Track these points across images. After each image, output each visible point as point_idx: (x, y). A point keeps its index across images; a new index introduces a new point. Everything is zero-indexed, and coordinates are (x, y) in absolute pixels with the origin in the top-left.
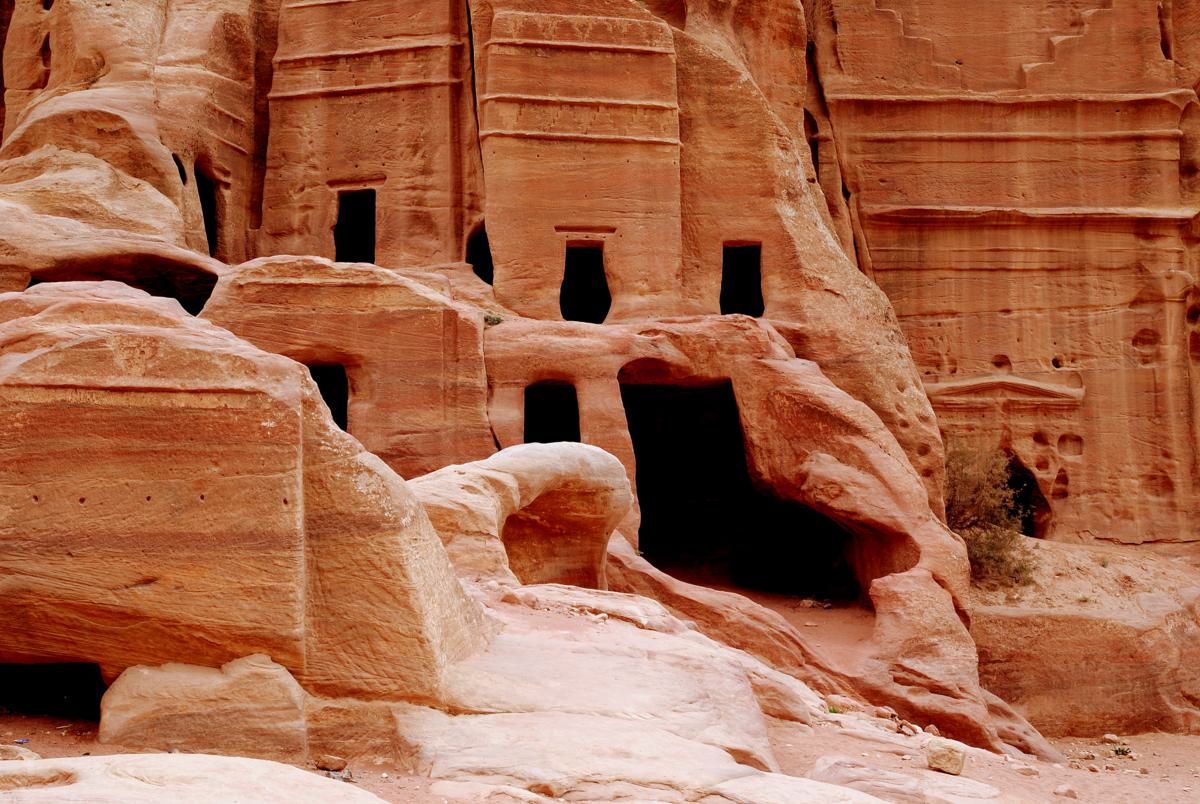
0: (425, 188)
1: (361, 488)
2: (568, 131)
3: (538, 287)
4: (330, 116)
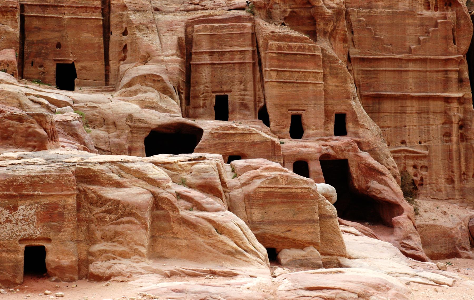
0: (245, 95)
1: (328, 208)
2: (291, 80)
3: (284, 128)
4: (212, 71)
